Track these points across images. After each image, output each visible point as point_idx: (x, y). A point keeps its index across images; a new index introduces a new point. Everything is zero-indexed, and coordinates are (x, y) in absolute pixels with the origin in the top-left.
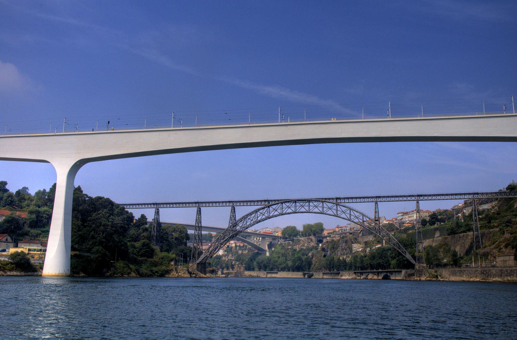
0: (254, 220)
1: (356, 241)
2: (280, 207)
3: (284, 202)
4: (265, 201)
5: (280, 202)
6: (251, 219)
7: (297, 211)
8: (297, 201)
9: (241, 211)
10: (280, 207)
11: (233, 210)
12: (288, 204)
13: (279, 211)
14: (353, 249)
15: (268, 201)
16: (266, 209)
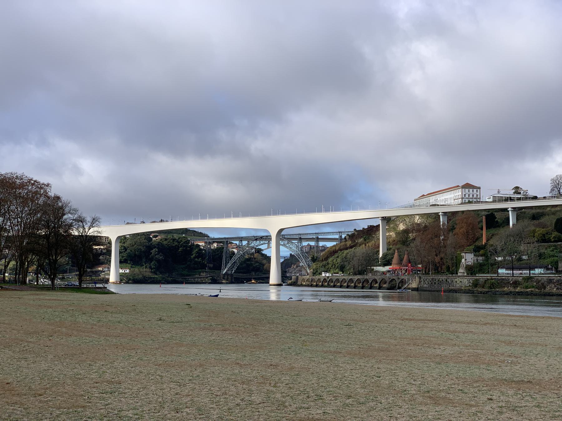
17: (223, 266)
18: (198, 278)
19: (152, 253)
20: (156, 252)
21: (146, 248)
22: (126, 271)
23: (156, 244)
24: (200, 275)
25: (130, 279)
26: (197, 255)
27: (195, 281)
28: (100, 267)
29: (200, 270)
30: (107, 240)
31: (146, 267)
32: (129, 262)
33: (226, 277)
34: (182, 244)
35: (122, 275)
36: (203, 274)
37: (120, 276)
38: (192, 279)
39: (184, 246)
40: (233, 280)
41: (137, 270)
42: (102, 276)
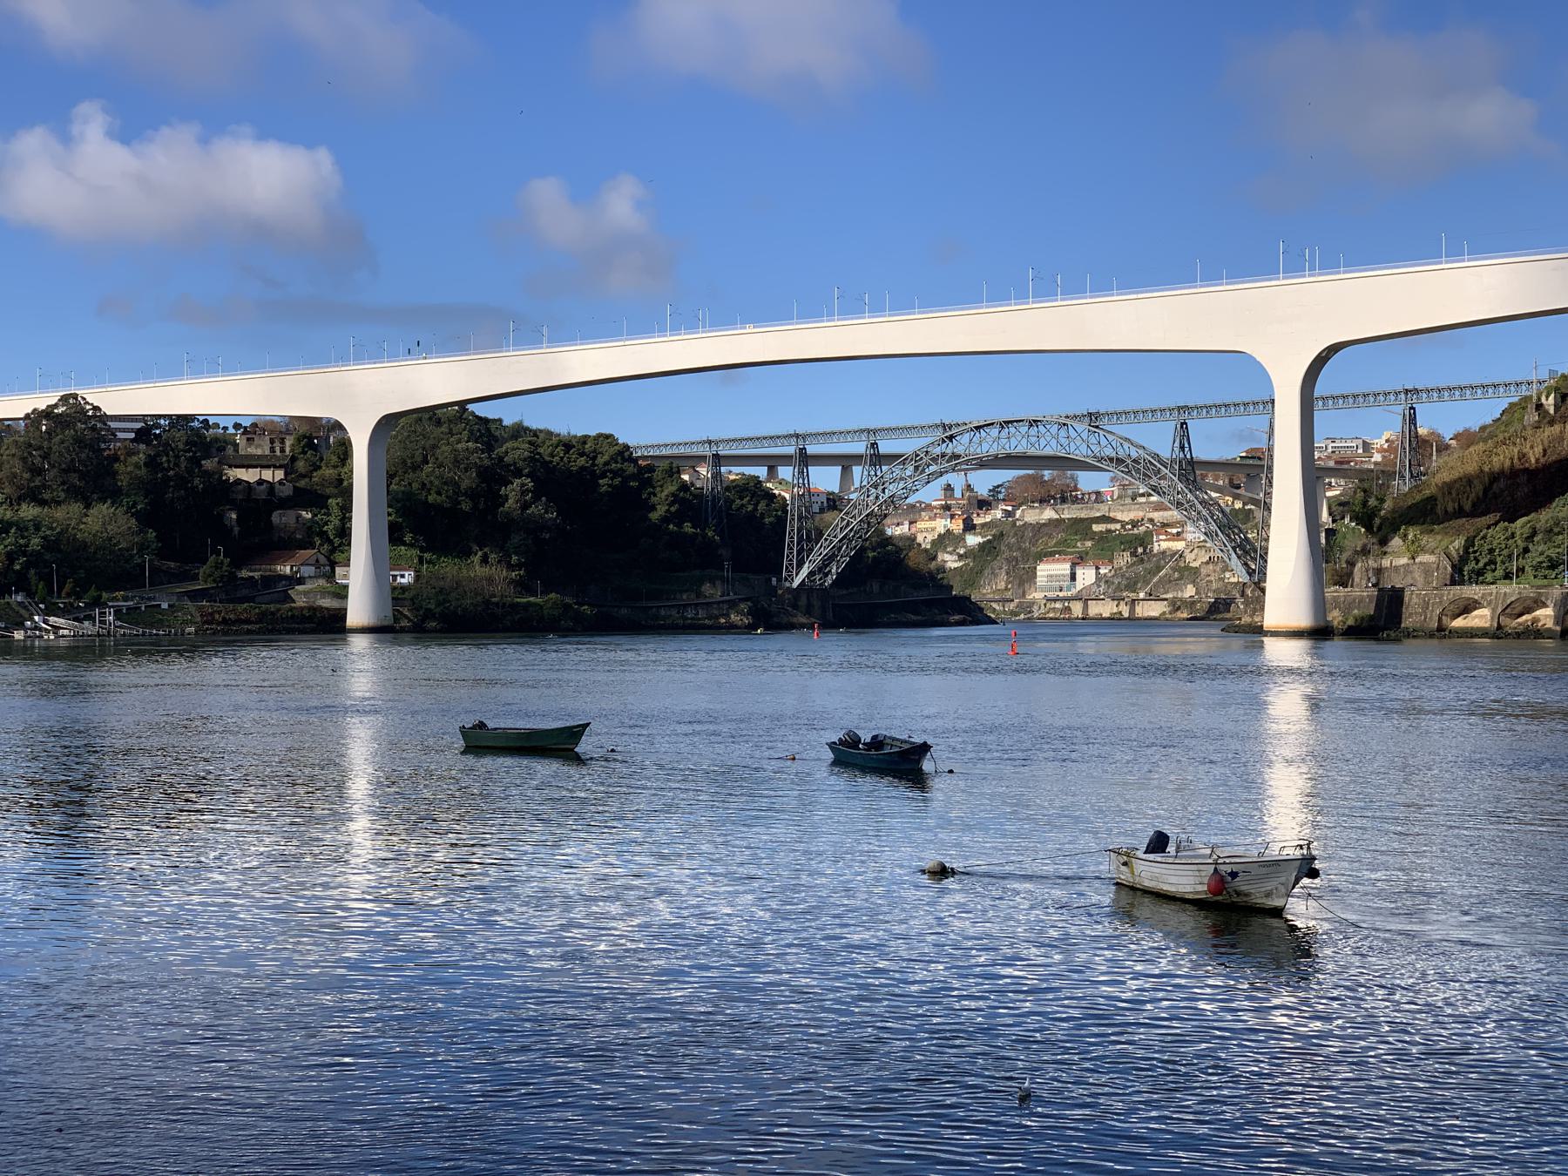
8: (1012, 422)
17: (790, 553)
19: (506, 498)
20: (528, 491)
21: (479, 474)
22: (403, 576)
23: (525, 460)
25: (429, 615)
26: (673, 509)
27: (688, 619)
28: (283, 563)
29: (697, 573)
30: (278, 449)
31: (485, 560)
32: (408, 538)
33: (803, 601)
34: (606, 464)
35: (399, 595)
36: (713, 592)
37: (393, 599)
38: (674, 612)
39: (615, 473)
40: (830, 615)
41: (449, 568)
42: (301, 597)
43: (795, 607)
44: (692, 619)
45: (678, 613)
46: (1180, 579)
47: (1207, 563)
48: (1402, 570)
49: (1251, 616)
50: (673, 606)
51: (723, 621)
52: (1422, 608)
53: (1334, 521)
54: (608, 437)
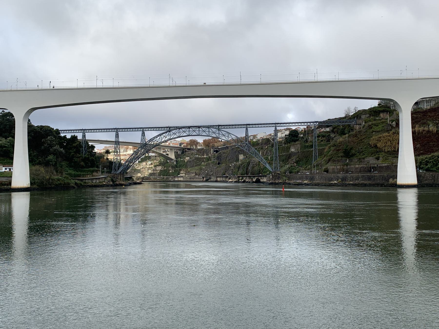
0: (159, 141)
1: (242, 152)
2: (178, 132)
3: (181, 128)
4: (167, 127)
5: (178, 128)
6: (157, 140)
7: (190, 134)
8: (191, 127)
9: (150, 135)
10: (178, 132)
11: (143, 134)
12: (184, 129)
13: (177, 134)
14: (240, 158)
15: (170, 127)
16: (168, 133)
18: (96, 179)
19: (44, 143)
24: (93, 176)
27: (94, 183)
29: (92, 169)
33: (119, 178)
38: (90, 181)
43: (118, 179)
44: (95, 183)
45: (91, 181)
46: (135, 172)
47: (143, 168)
48: (384, 168)
49: (275, 180)
50: (90, 179)
51: (105, 183)
52: (432, 178)
53: (176, 159)
54: (49, 127)
